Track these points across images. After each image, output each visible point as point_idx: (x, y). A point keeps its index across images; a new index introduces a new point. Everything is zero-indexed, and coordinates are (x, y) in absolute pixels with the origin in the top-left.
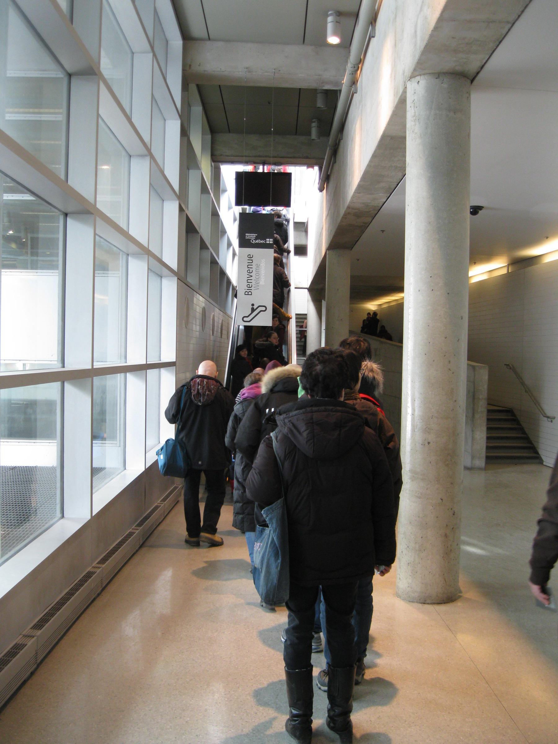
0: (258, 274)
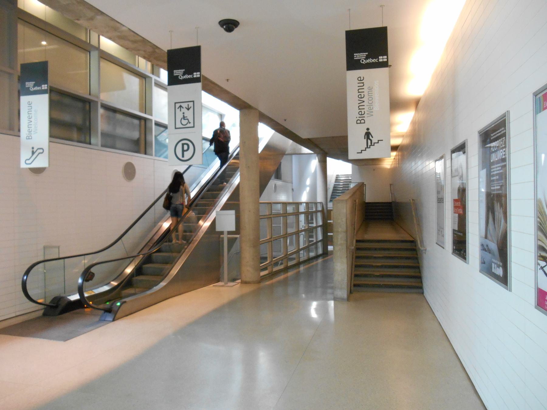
0: (371, 98)
